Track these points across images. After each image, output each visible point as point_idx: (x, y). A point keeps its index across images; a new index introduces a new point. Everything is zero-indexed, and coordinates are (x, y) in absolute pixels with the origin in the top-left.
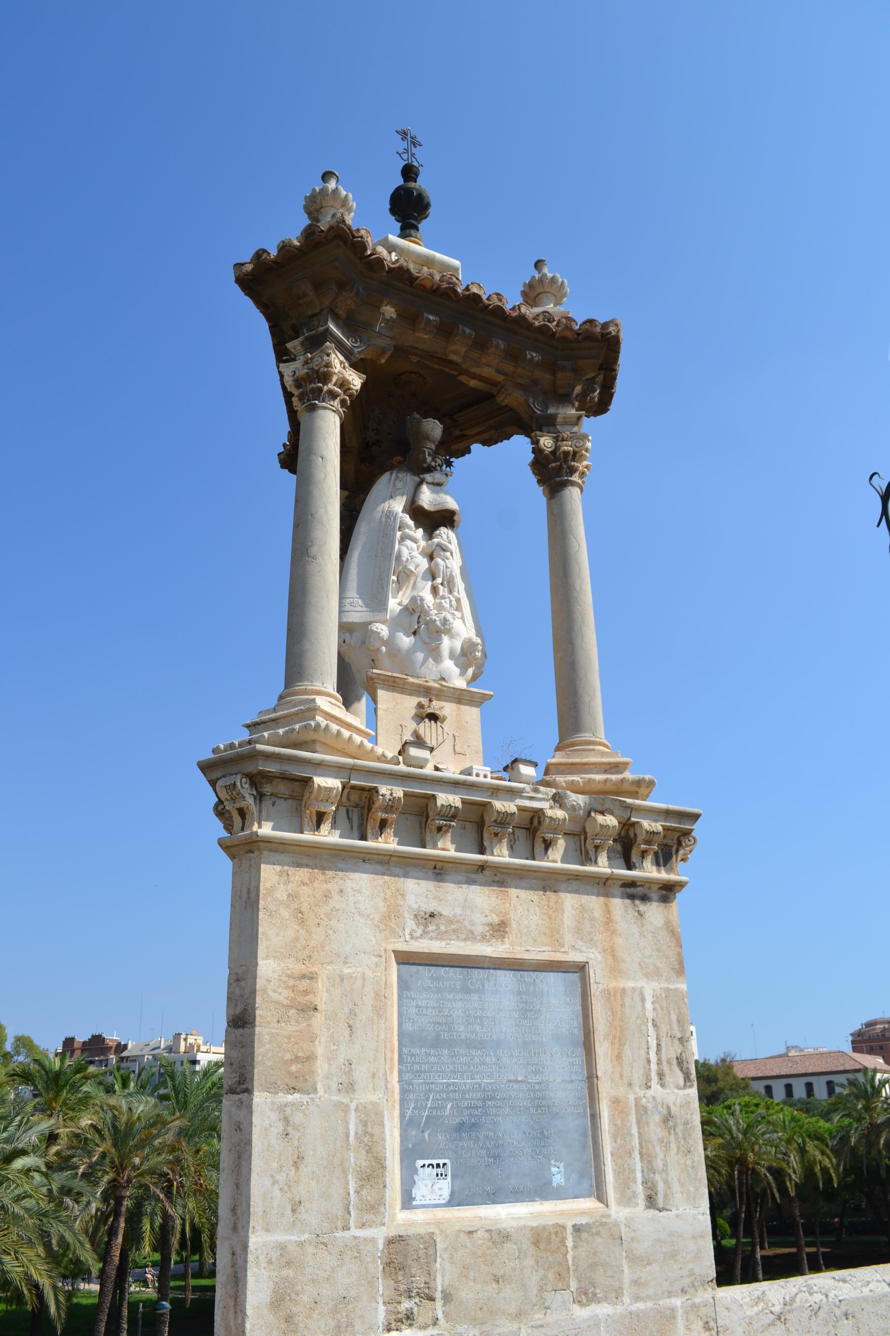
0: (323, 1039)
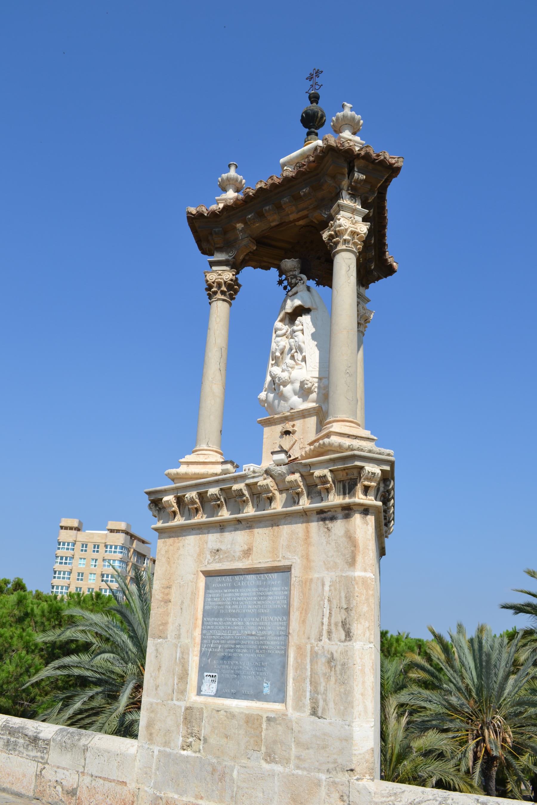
0: (171, 615)
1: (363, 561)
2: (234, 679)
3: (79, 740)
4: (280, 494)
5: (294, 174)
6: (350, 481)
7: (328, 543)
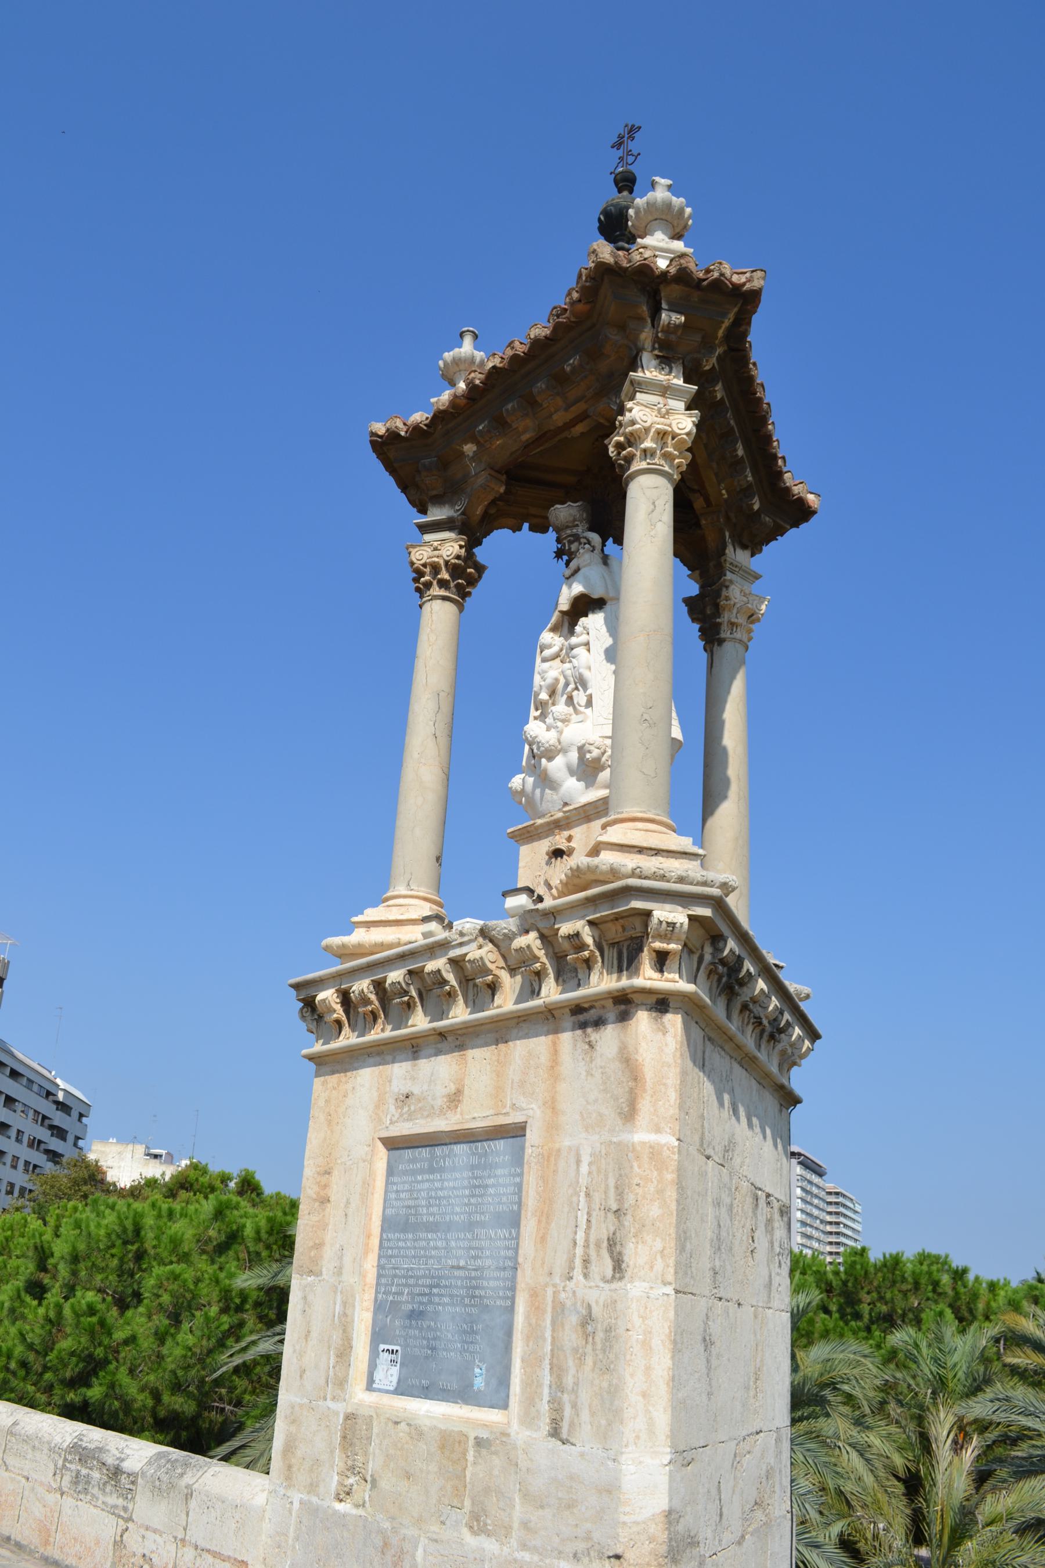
0: (330, 1227)
1: (652, 1109)
2: (427, 1357)
3: (182, 1475)
4: (511, 977)
5: (548, 332)
6: (629, 942)
7: (589, 1074)
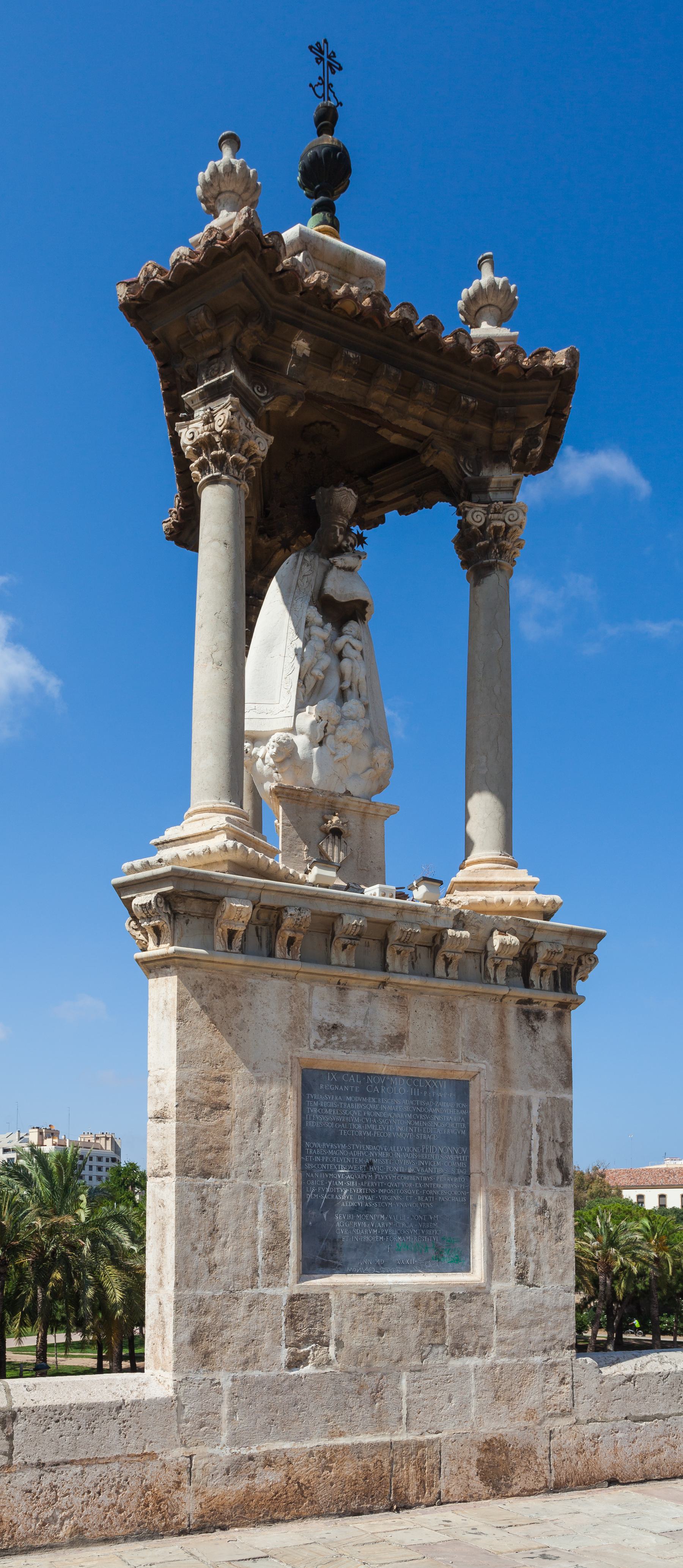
7: (533, 1049)
